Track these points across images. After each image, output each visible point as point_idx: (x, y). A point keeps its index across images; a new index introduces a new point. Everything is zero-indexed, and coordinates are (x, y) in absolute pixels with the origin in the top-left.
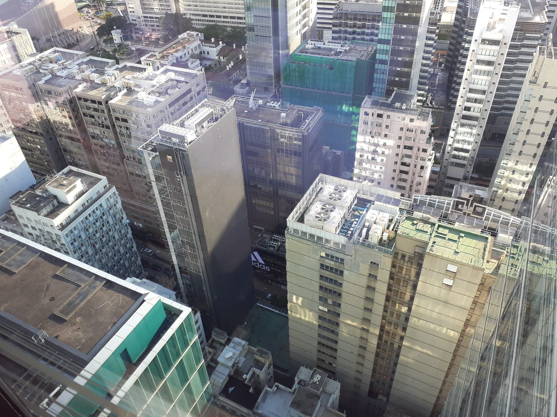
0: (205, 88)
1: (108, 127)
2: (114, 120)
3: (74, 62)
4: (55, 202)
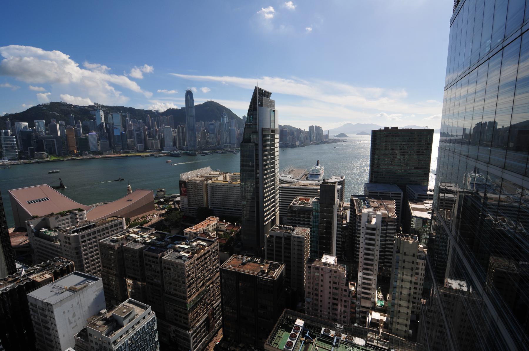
0: (218, 249)
1: (158, 272)
2: (163, 268)
3: (147, 233)
4: (115, 324)
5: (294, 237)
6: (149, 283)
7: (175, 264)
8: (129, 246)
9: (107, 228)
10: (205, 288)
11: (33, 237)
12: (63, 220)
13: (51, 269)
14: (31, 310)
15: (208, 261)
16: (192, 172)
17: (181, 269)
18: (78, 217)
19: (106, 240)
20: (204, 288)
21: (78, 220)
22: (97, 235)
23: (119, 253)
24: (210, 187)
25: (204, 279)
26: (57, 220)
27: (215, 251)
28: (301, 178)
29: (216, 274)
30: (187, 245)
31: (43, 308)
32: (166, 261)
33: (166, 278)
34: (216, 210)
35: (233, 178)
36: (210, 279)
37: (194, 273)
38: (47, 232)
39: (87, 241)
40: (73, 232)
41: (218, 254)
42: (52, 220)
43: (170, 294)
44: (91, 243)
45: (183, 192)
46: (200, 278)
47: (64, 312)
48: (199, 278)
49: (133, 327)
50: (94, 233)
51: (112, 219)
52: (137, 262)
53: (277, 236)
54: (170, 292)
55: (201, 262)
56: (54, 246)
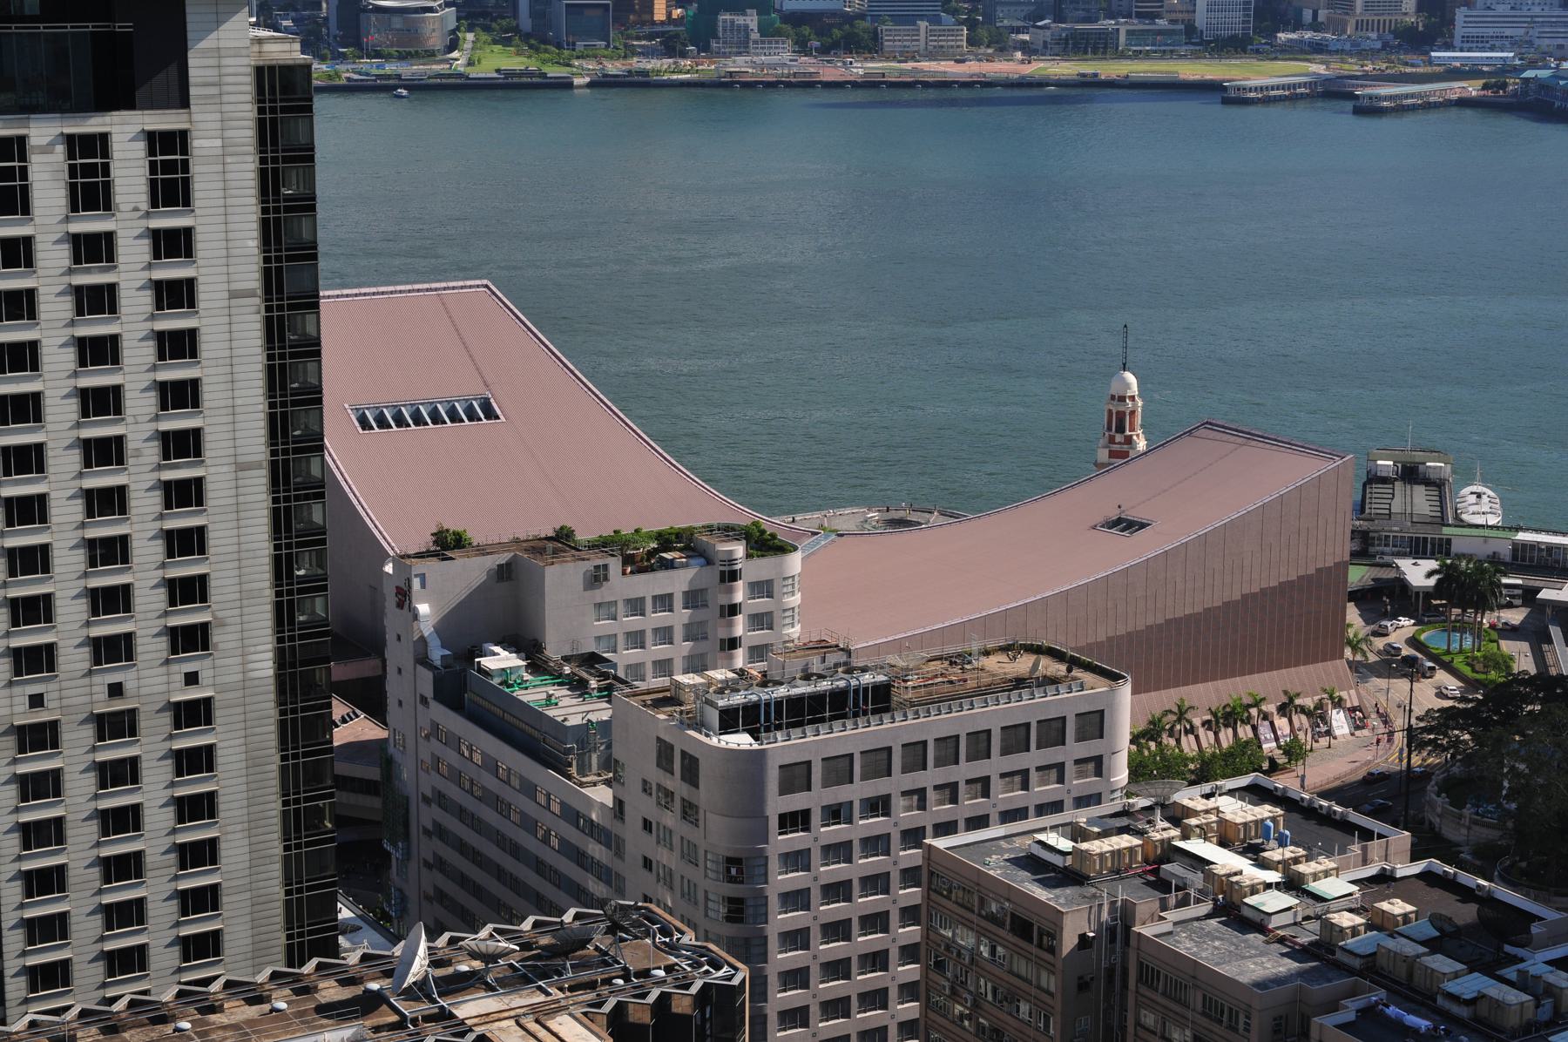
8: (1185, 946)
9: (980, 744)
11: (424, 701)
12: (636, 606)
13: (591, 986)
18: (739, 596)
21: (740, 626)
22: (895, 783)
23: (1083, 986)
26: (603, 594)
38: (523, 684)
39: (816, 818)
40: (729, 721)
44: (839, 851)
50: (879, 763)
51: (1024, 664)
56: (573, 815)
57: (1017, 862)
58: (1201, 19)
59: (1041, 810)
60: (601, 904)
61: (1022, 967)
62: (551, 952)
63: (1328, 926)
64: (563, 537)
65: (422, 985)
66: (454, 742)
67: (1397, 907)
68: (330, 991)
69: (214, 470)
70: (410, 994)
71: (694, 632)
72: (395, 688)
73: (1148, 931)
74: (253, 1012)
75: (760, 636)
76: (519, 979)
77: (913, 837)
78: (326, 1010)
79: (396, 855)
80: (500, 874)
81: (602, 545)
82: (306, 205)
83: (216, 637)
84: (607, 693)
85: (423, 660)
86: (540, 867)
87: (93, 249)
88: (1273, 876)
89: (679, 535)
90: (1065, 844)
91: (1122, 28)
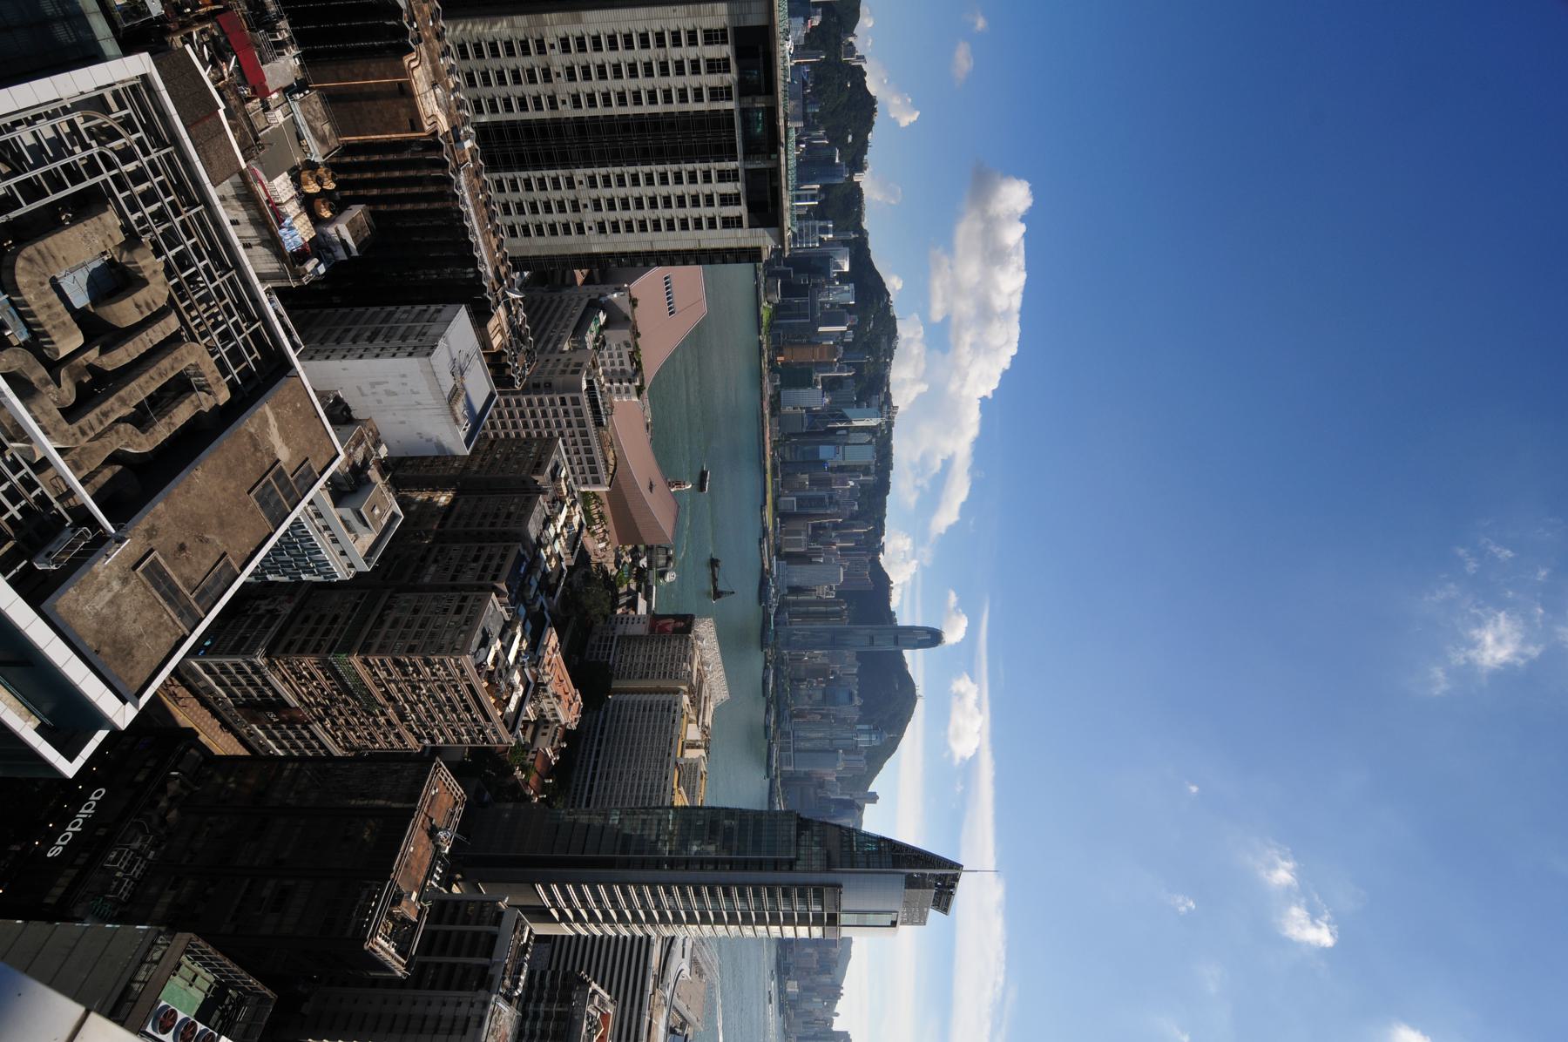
0: (488, 743)
1: (454, 578)
4: (348, 489)
5: (485, 1004)
6: (429, 550)
7: (471, 629)
8: (537, 509)
9: (588, 451)
10: (380, 705)
12: (620, 356)
13: (511, 345)
14: (424, 307)
15: (458, 716)
16: (717, 650)
17: (452, 642)
18: (624, 384)
19: (560, 453)
20: (381, 700)
21: (616, 384)
22: (577, 430)
23: (524, 482)
24: (670, 701)
25: (407, 701)
26: (623, 346)
27: (484, 734)
28: (677, 1011)
29: (414, 733)
30: (517, 658)
31: (425, 334)
32: (482, 602)
33: (435, 598)
34: (598, 717)
35: (690, 774)
36: (402, 717)
37: (433, 678)
38: (596, 324)
39: (564, 407)
40: (590, 382)
41: (473, 741)
42: (625, 334)
43: (388, 607)
44: (556, 414)
45: (661, 622)
46: (414, 692)
47: (404, 376)
48: (415, 688)
49: (327, 528)
50: (582, 424)
51: (611, 462)
52: (493, 524)
53: (499, 941)
54: (390, 608)
55: (461, 696)
56: (560, 340)
57: (557, 463)
58: (782, 499)
59: (572, 469)
60: (535, 348)
61: (527, 465)
62: (520, 334)
63: (547, 546)
64: (638, 335)
65: (507, 297)
66: (578, 304)
67: (553, 563)
68: (503, 270)
69: (650, 235)
70: (504, 293)
71: (614, 372)
72: (592, 288)
73: (541, 498)
74: (495, 247)
75: (614, 390)
76: (511, 324)
77: (561, 434)
78: (497, 268)
79: (544, 289)
80: (541, 319)
81: (636, 345)
82: (725, 261)
83: (603, 235)
84: (595, 348)
85: (601, 296)
86: (544, 330)
87: (709, 201)
88: (559, 531)
89: (641, 367)
90: (563, 475)
91: (779, 479)
